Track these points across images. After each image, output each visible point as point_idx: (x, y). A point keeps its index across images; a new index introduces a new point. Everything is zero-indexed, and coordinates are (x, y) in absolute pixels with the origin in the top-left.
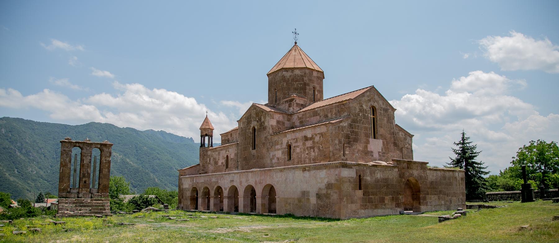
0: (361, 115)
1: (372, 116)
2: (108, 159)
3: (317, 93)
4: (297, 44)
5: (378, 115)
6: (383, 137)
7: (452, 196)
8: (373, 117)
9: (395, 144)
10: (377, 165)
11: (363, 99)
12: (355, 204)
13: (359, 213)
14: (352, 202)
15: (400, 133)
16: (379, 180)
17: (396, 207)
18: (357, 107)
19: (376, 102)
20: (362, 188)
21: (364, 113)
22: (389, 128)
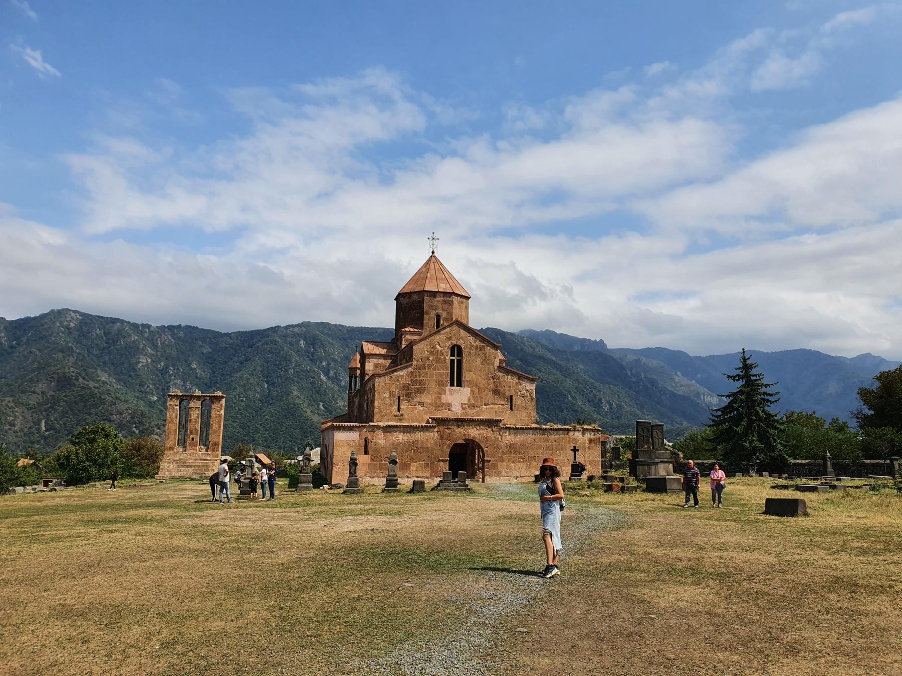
0: (431, 358)
2: (218, 413)
3: (442, 322)
4: (435, 254)
5: (464, 355)
6: (470, 383)
7: (564, 465)
8: (458, 358)
9: (496, 392)
10: (397, 425)
11: (437, 338)
16: (400, 442)
17: (431, 476)
19: (462, 339)
20: (370, 452)
21: (437, 355)
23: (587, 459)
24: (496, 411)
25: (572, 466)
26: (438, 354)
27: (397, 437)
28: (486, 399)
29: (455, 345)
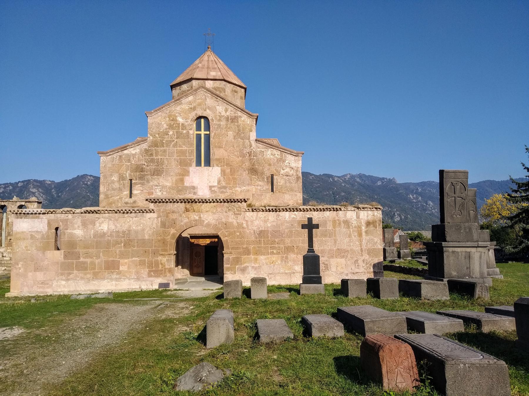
0: (171, 133)
1: (203, 133)
5: (211, 129)
6: (220, 161)
7: (332, 257)
9: (253, 171)
11: (178, 108)
12: (42, 273)
13: (53, 285)
14: (37, 269)
17: (150, 276)
18: (163, 123)
19: (209, 108)
21: (179, 129)
22: (238, 146)
23: (364, 247)
24: (253, 195)
25: (306, 259)
26: (179, 127)
27: (100, 226)
28: (240, 180)
29: (200, 118)
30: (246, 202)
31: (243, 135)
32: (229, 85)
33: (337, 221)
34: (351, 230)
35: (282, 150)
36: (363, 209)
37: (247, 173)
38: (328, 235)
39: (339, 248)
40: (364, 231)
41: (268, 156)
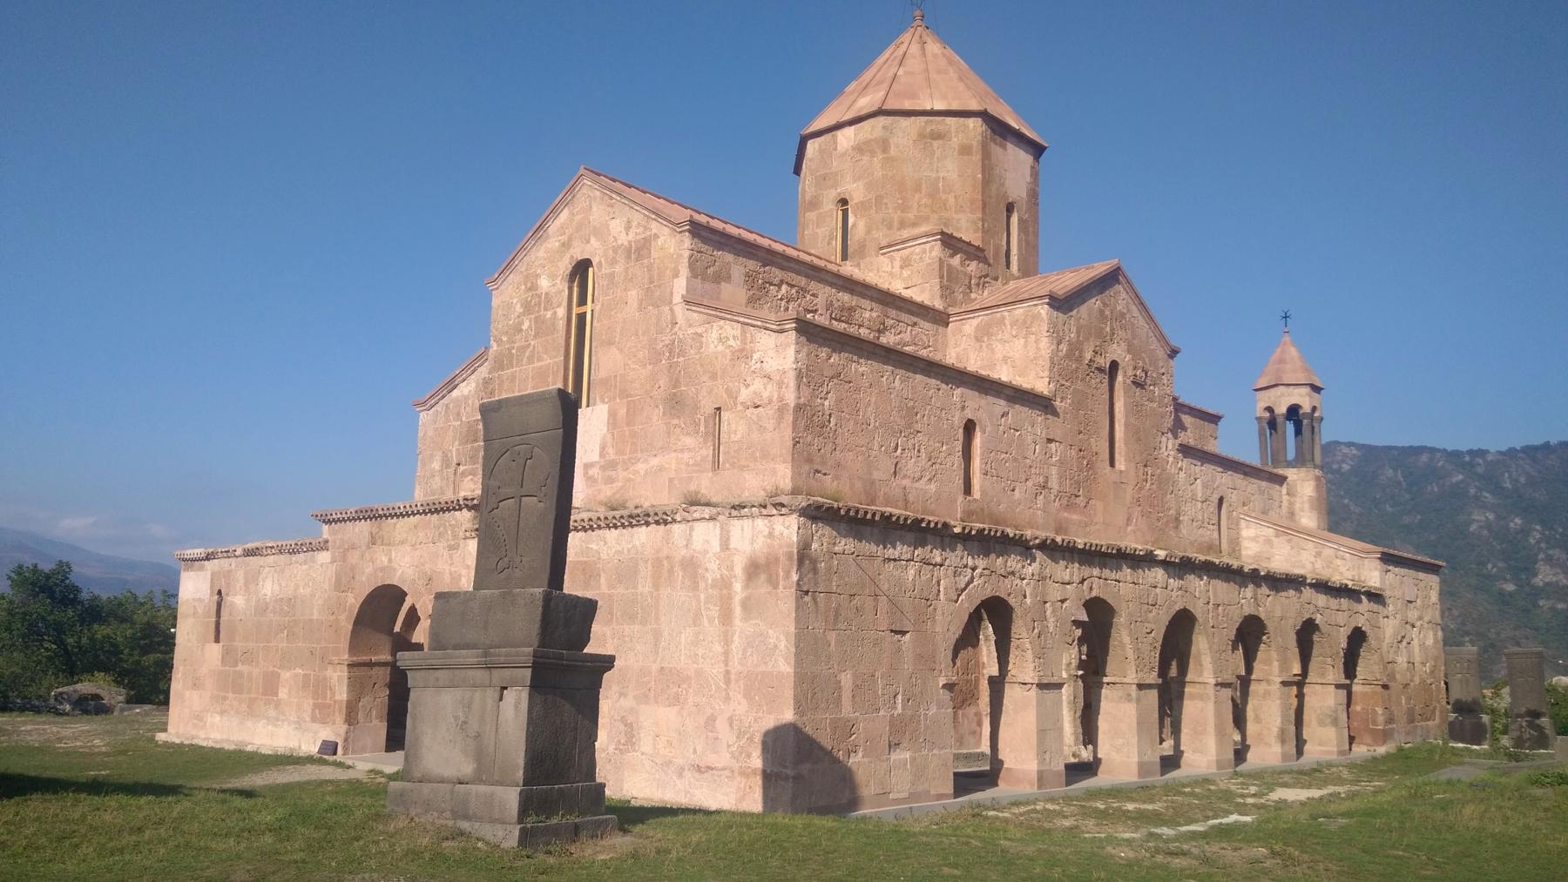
7: (644, 698)
9: (676, 404)
15: (714, 335)
18: (515, 301)
21: (539, 311)
23: (735, 665)
30: (469, 508)
31: (658, 293)
32: (905, 122)
33: (665, 563)
34: (702, 596)
35: (742, 319)
36: (734, 513)
37: (662, 410)
38: (639, 616)
39: (662, 665)
40: (737, 599)
41: (712, 346)
